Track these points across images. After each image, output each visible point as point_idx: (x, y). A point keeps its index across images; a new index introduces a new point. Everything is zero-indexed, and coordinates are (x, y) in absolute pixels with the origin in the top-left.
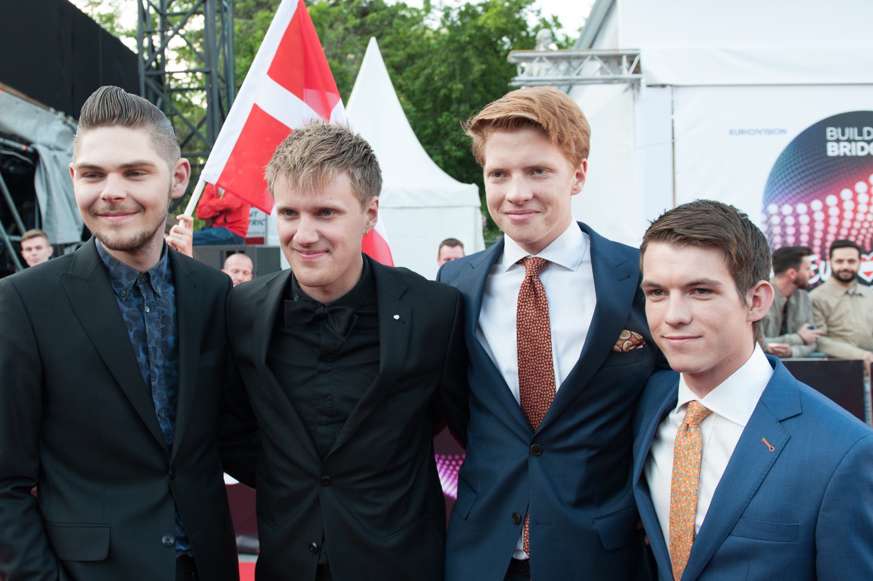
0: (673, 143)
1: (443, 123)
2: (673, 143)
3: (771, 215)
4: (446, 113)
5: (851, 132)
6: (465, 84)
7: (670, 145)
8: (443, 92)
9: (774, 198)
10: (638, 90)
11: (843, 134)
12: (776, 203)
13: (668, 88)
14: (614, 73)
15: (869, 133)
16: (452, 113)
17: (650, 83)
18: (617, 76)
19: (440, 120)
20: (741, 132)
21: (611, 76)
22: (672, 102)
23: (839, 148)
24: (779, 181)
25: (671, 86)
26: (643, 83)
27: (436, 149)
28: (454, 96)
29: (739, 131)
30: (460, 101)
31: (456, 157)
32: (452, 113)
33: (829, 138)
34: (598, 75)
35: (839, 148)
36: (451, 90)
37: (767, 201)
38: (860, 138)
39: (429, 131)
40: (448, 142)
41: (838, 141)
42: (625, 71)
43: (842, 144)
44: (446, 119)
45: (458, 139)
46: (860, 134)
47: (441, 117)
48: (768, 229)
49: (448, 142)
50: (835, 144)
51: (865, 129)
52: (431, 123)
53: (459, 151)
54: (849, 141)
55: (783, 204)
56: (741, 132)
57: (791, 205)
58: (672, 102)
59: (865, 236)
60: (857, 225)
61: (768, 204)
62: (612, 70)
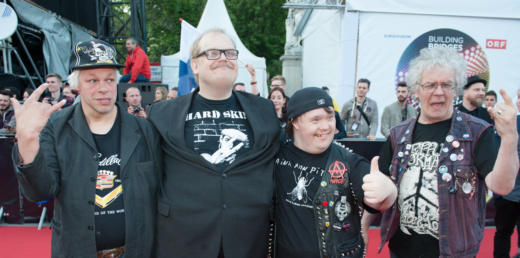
0: (358, 40)
1: (250, 27)
2: (358, 40)
3: (400, 77)
4: (252, 22)
5: (440, 39)
6: (261, 7)
7: (356, 41)
8: (250, 10)
9: (402, 69)
10: (344, 13)
11: (436, 40)
12: (403, 71)
13: (358, 12)
14: (333, 4)
15: (448, 40)
16: (255, 22)
17: (349, 10)
18: (334, 5)
19: (249, 25)
20: (390, 36)
21: (331, 5)
22: (359, 19)
23: (434, 46)
24: (405, 61)
25: (359, 11)
26: (346, 9)
27: (247, 40)
28: (256, 13)
29: (389, 35)
30: (259, 16)
31: (256, 44)
32: (255, 22)
33: (430, 41)
34: (325, 4)
35: (434, 46)
36: (255, 10)
37: (398, 70)
38: (444, 42)
39: (243, 31)
40: (252, 36)
41: (433, 43)
42: (338, 3)
43: (435, 44)
44: (251, 25)
45: (257, 35)
46: (444, 40)
47: (249, 24)
49: (252, 36)
50: (432, 44)
51: (447, 38)
52: (244, 27)
53: (257, 41)
54: (438, 43)
56: (390, 36)
58: (359, 19)
61: (399, 72)
62: (331, 2)
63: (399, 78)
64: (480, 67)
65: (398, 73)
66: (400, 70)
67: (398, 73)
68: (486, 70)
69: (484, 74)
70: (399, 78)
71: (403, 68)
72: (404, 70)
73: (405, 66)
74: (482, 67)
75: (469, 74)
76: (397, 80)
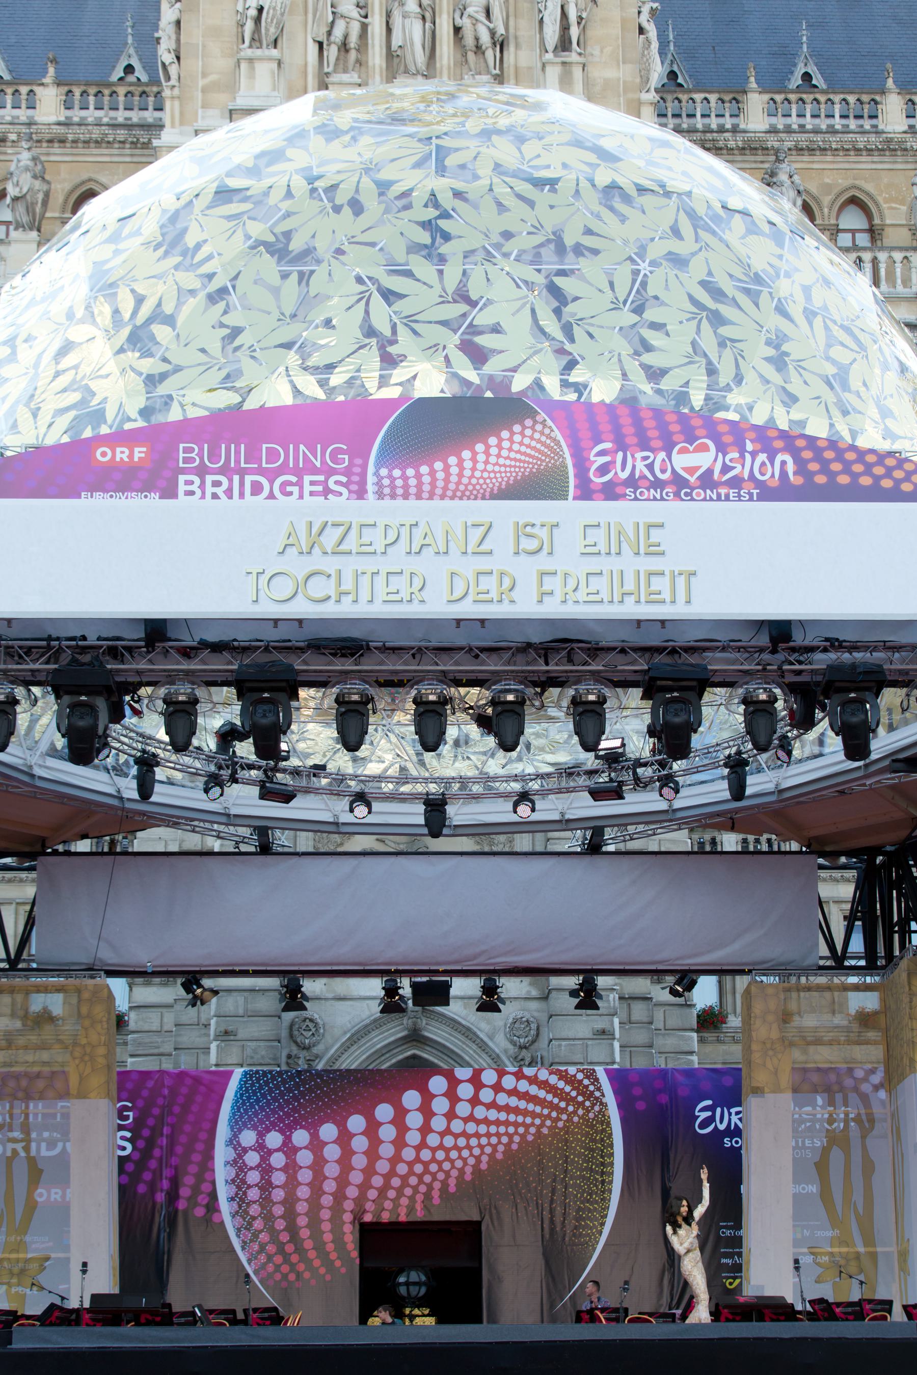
3: (245, 1150)
12: (254, 1128)
24: (261, 1088)
48: (237, 1175)
55: (268, 1130)
57: (281, 1131)
59: (415, 1189)
60: (402, 1169)
61: (240, 1131)
63: (240, 1156)
64: (570, 1100)
65: (235, 1136)
66: (245, 1125)
67: (235, 1136)
68: (597, 1108)
69: (592, 1127)
70: (240, 1156)
71: (256, 1114)
72: (261, 1122)
73: (262, 1109)
74: (580, 1099)
75: (527, 1127)
76: (235, 1161)
